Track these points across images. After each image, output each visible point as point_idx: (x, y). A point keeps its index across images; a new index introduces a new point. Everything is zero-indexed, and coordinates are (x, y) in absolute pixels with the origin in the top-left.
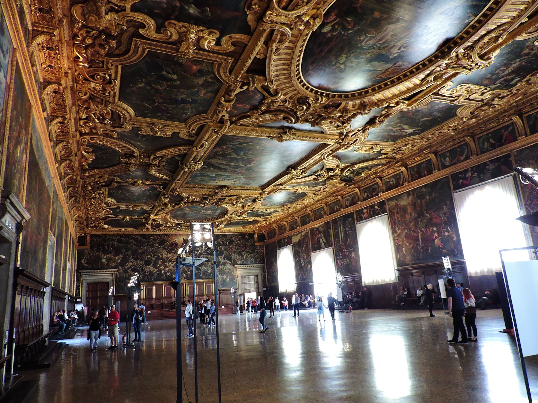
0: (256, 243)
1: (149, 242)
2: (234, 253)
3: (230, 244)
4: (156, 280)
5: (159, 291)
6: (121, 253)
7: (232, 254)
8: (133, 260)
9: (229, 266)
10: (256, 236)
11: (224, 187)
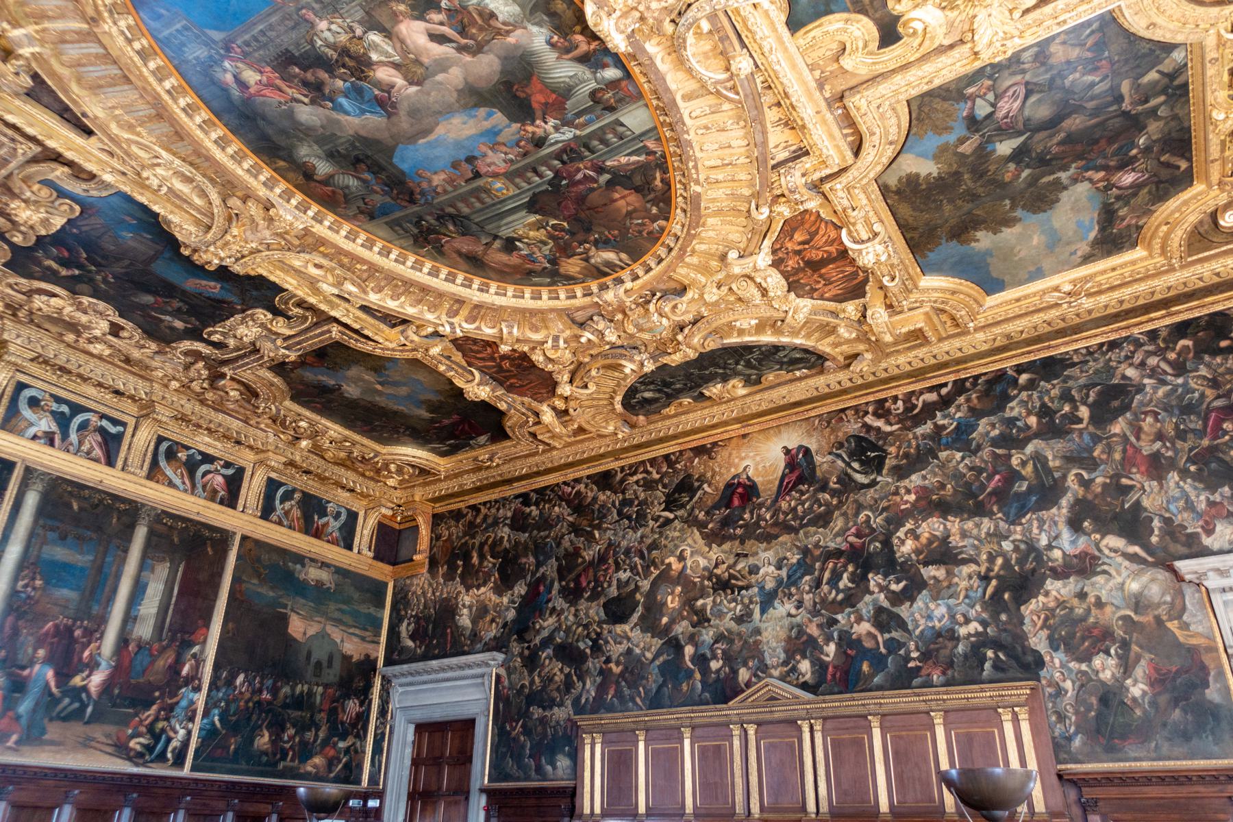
2: (1157, 467)
3: (1102, 415)
4: (655, 702)
6: (521, 573)
7: (1137, 478)
8: (560, 603)
9: (1123, 580)
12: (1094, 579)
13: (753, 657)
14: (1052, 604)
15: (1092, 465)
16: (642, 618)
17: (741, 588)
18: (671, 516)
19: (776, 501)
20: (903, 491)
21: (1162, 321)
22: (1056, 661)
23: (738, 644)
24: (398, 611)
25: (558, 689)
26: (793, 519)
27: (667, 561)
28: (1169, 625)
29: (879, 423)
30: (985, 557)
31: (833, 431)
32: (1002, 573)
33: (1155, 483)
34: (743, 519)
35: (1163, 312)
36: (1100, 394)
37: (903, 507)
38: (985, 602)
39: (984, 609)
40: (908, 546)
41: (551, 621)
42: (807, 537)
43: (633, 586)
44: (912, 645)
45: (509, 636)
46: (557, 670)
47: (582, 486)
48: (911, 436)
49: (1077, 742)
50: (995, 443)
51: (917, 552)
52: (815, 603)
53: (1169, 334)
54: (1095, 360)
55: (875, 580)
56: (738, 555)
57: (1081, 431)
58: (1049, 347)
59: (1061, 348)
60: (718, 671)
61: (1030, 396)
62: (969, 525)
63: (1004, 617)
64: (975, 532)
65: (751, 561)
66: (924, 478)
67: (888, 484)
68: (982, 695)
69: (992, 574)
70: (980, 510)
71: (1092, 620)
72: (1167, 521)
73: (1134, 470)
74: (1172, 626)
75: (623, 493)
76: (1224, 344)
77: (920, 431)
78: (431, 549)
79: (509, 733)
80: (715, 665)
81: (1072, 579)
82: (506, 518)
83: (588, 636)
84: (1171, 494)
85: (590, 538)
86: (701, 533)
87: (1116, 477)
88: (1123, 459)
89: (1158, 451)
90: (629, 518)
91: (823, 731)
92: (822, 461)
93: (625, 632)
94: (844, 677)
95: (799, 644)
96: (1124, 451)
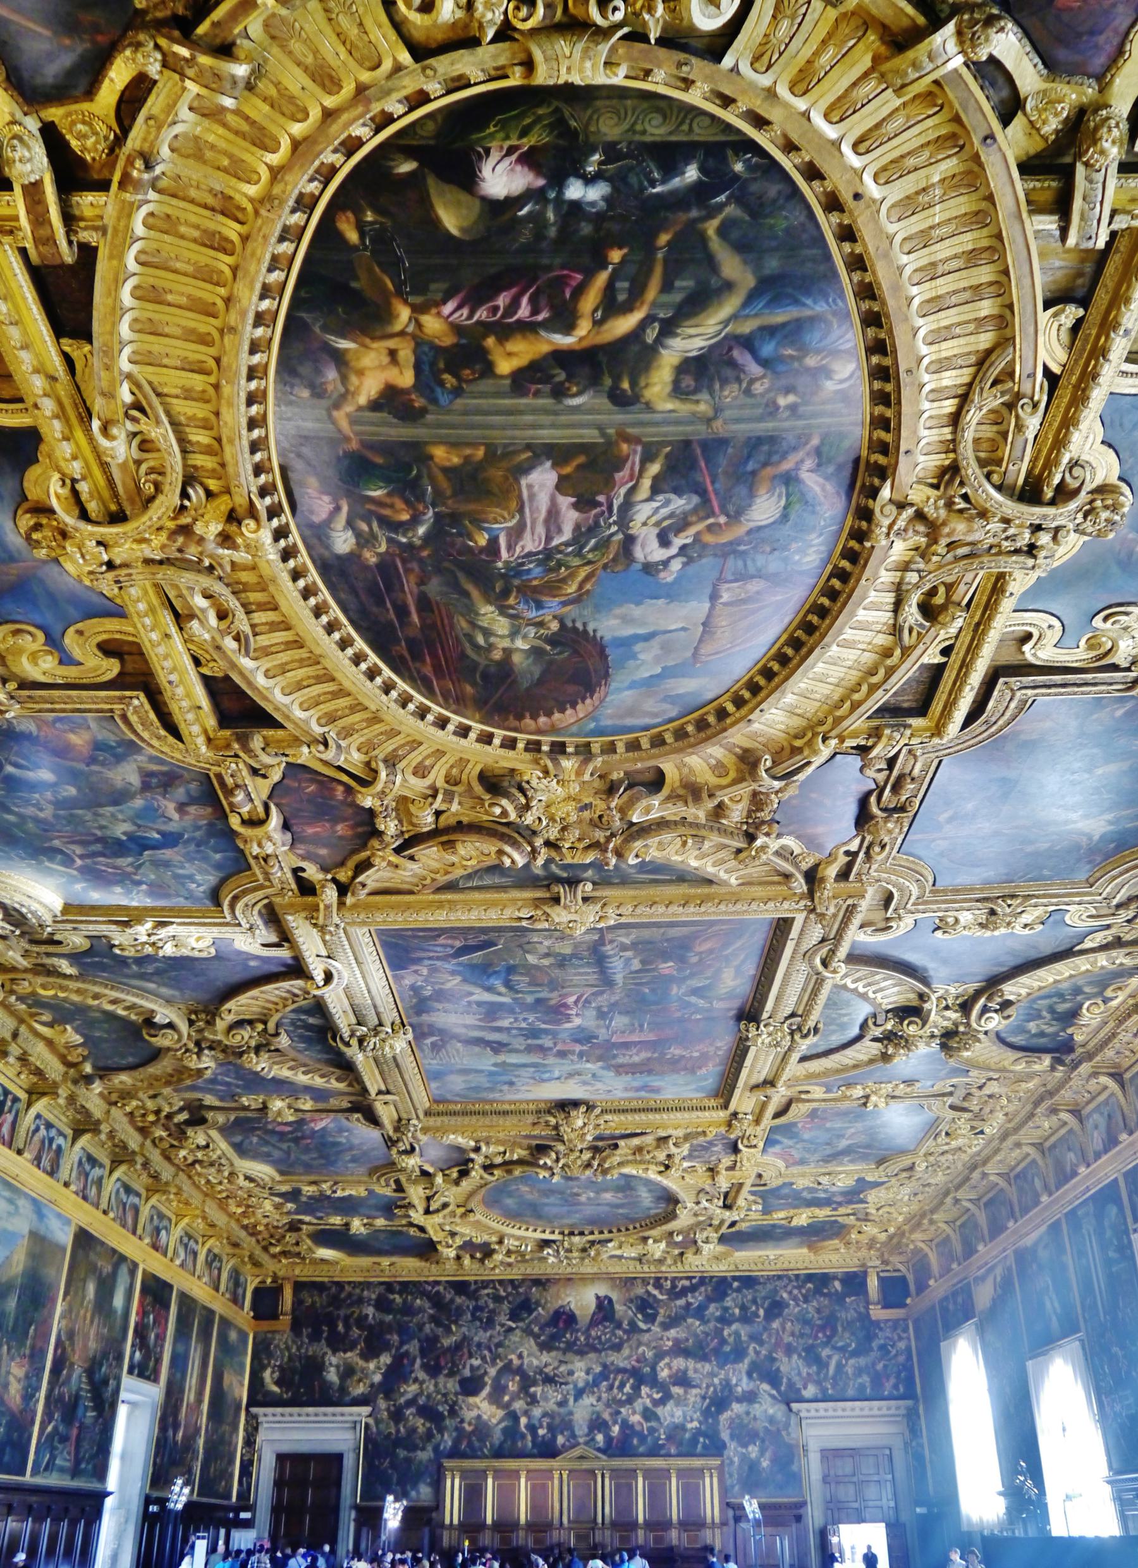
0: (877, 1313)
1: (477, 1308)
2: (789, 1350)
3: (771, 1315)
4: (498, 1454)
5: (506, 1497)
6: (387, 1347)
7: (779, 1355)
8: (422, 1375)
9: (767, 1408)
10: (873, 1283)
11: (576, 1104)
15: (761, 1343)
22: (732, 1447)
23: (557, 1421)
24: (260, 1360)
29: (656, 1292)
41: (412, 1389)
46: (421, 1425)
55: (645, 1390)
68: (697, 1463)
70: (705, 1358)
78: (294, 1309)
80: (541, 1432)
85: (449, 1331)
92: (619, 1308)
95: (597, 1424)
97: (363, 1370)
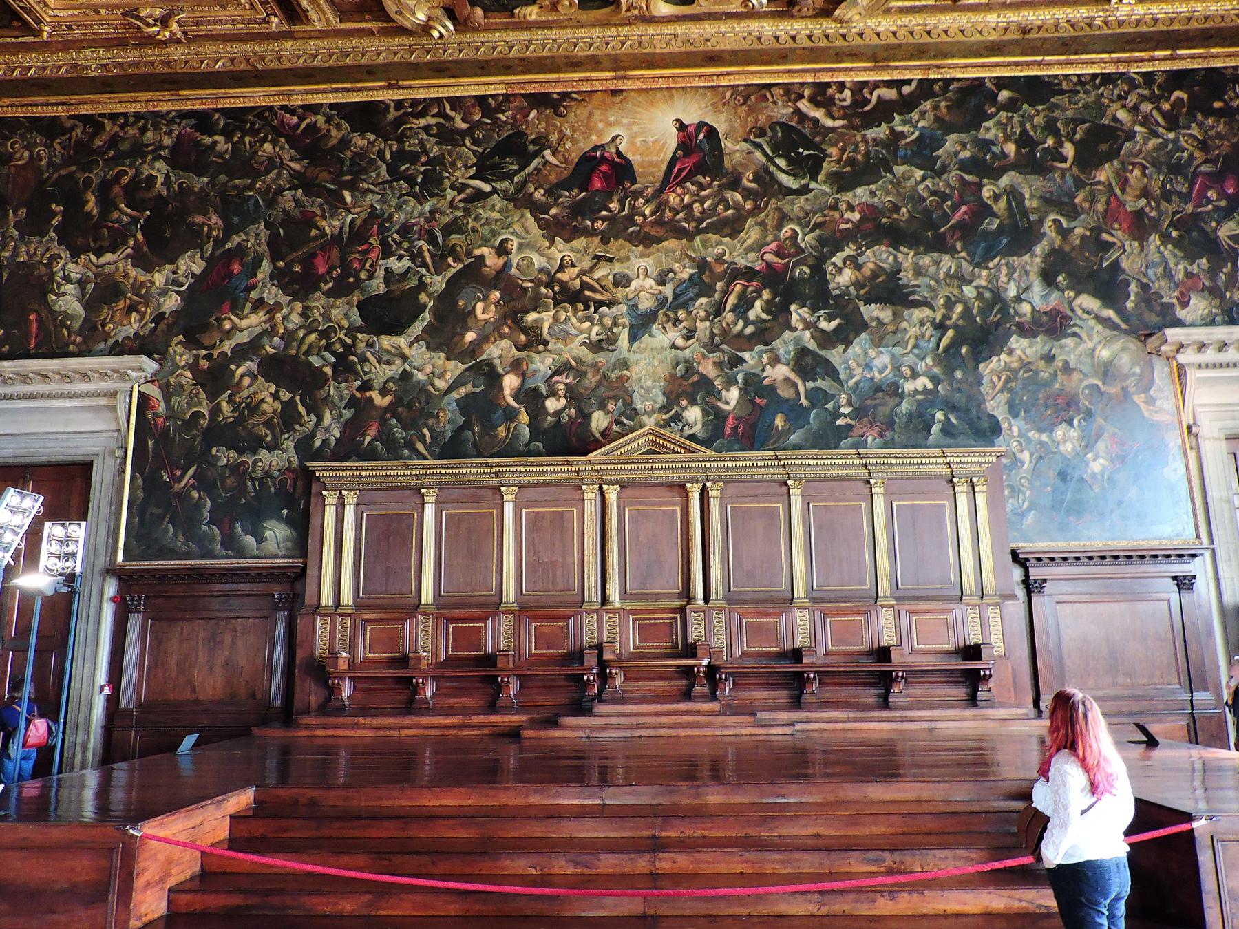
2: (1140, 226)
3: (1088, 158)
4: (451, 449)
5: (469, 538)
6: (194, 239)
7: (1117, 235)
8: (273, 294)
9: (1094, 343)
12: (1063, 341)
13: (616, 399)
14: (1015, 365)
15: (1073, 212)
16: (428, 330)
17: (599, 304)
18: (487, 188)
19: (661, 190)
20: (843, 206)
21: (1160, 62)
22: (1013, 427)
23: (591, 380)
25: (268, 424)
26: (686, 220)
27: (477, 252)
28: (1135, 398)
29: (818, 114)
30: (942, 301)
31: (751, 111)
32: (961, 322)
33: (1136, 244)
34: (609, 210)
35: (1168, 53)
36: (1087, 132)
37: (843, 226)
38: (938, 355)
39: (936, 363)
40: (846, 277)
41: (253, 322)
42: (705, 247)
43: (414, 282)
44: (843, 398)
45: (169, 333)
46: (268, 397)
47: (320, 120)
48: (859, 138)
49: (1030, 519)
50: (964, 166)
51: (858, 285)
52: (713, 335)
53: (1165, 81)
54: (1086, 92)
55: (798, 313)
56: (597, 257)
57: (1063, 170)
58: (1039, 64)
59: (1055, 68)
60: (558, 413)
61: (1010, 119)
62: (926, 260)
63: (958, 374)
64: (932, 270)
65: (618, 268)
66: (873, 194)
67: (824, 194)
69: (948, 323)
70: (940, 245)
71: (1057, 386)
72: (1145, 287)
73: (1116, 226)
74: (1139, 399)
75: (400, 140)
76: (1217, 105)
77: (871, 133)
79: (169, 486)
80: (552, 405)
81: (1039, 339)
82: (163, 148)
83: (328, 348)
84: (1150, 258)
86: (537, 220)
87: (1097, 230)
88: (1106, 211)
89: (1142, 209)
90: (411, 180)
91: (721, 498)
93: (398, 348)
94: (752, 431)
95: (686, 385)
96: (1108, 203)
97: (137, 287)
